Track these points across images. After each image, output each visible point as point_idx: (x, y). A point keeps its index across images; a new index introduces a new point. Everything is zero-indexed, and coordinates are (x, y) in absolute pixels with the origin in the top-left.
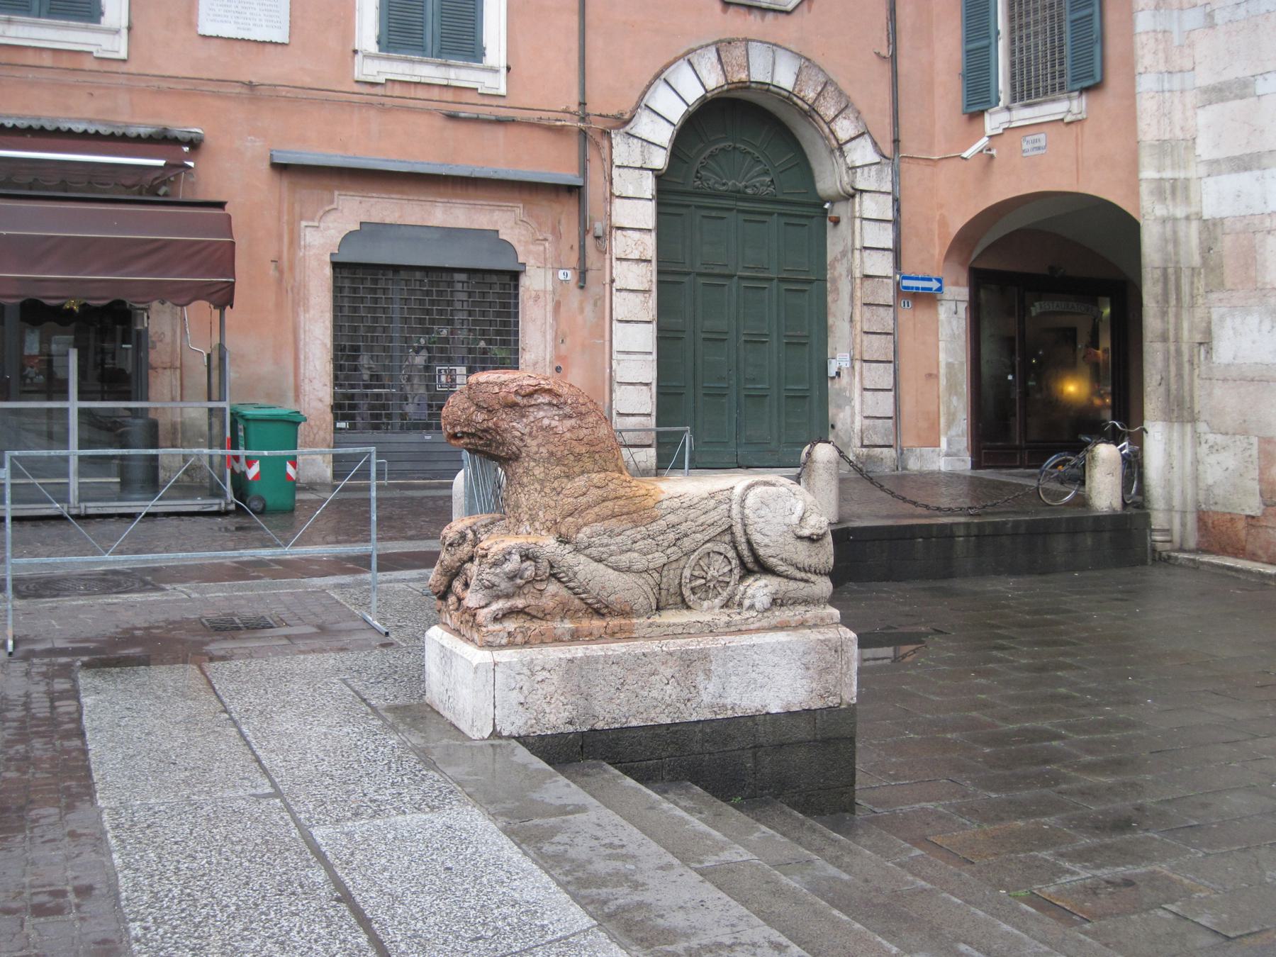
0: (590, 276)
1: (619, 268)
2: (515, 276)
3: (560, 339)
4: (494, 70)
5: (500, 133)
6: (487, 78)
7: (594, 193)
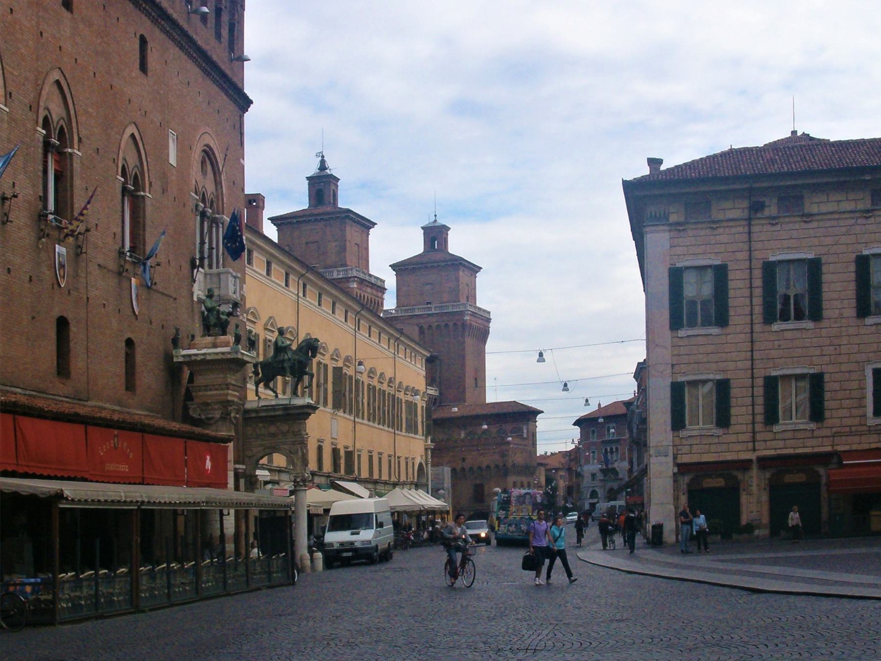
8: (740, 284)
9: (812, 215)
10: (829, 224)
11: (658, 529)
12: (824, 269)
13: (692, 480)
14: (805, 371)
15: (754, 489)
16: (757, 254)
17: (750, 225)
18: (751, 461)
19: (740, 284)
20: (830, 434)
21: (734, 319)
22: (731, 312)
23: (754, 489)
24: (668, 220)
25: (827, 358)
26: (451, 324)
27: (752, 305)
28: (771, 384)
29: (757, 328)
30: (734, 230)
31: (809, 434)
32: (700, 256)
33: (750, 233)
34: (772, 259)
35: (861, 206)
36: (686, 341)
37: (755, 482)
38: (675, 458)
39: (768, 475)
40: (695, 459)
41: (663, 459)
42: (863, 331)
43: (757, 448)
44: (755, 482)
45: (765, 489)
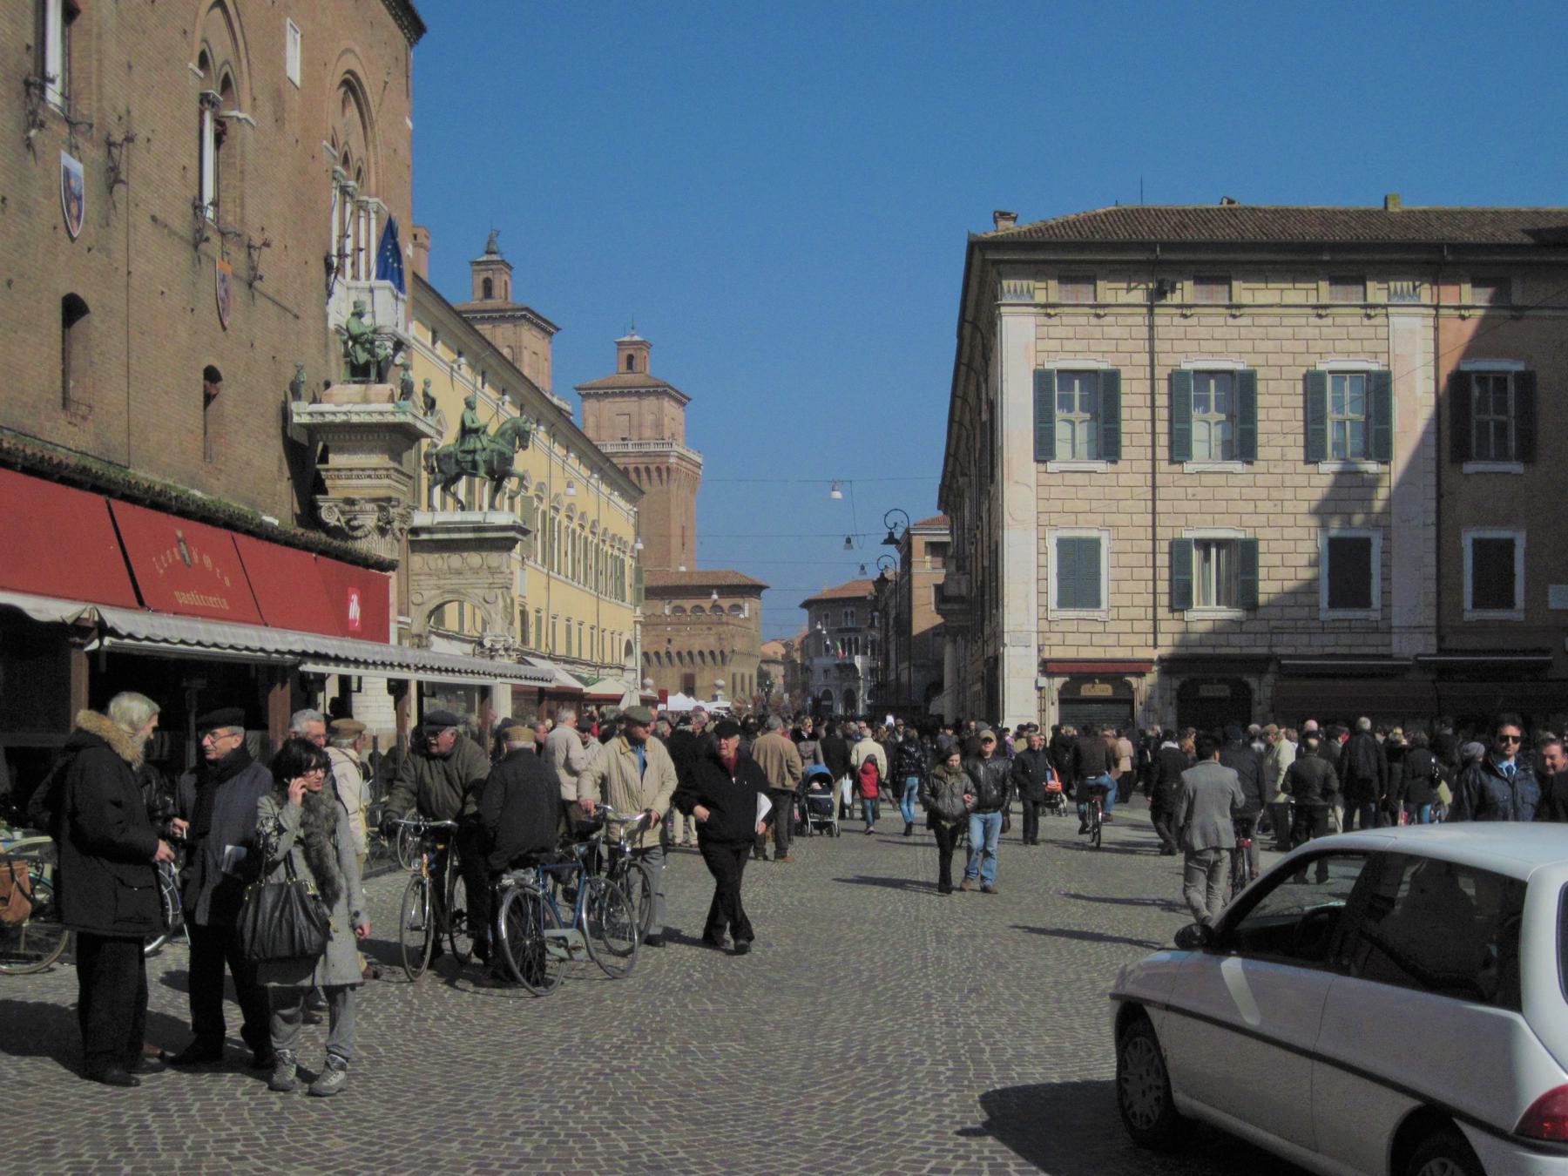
10: (1264, 321)
12: (1260, 387)
14: (1231, 534)
16: (1161, 359)
17: (1151, 314)
24: (1032, 297)
25: (1263, 518)
26: (653, 468)
28: (1180, 550)
29: (1163, 466)
30: (1130, 321)
32: (1079, 356)
33: (1151, 327)
34: (1186, 367)
36: (1058, 479)
39: (1176, 683)
40: (1070, 653)
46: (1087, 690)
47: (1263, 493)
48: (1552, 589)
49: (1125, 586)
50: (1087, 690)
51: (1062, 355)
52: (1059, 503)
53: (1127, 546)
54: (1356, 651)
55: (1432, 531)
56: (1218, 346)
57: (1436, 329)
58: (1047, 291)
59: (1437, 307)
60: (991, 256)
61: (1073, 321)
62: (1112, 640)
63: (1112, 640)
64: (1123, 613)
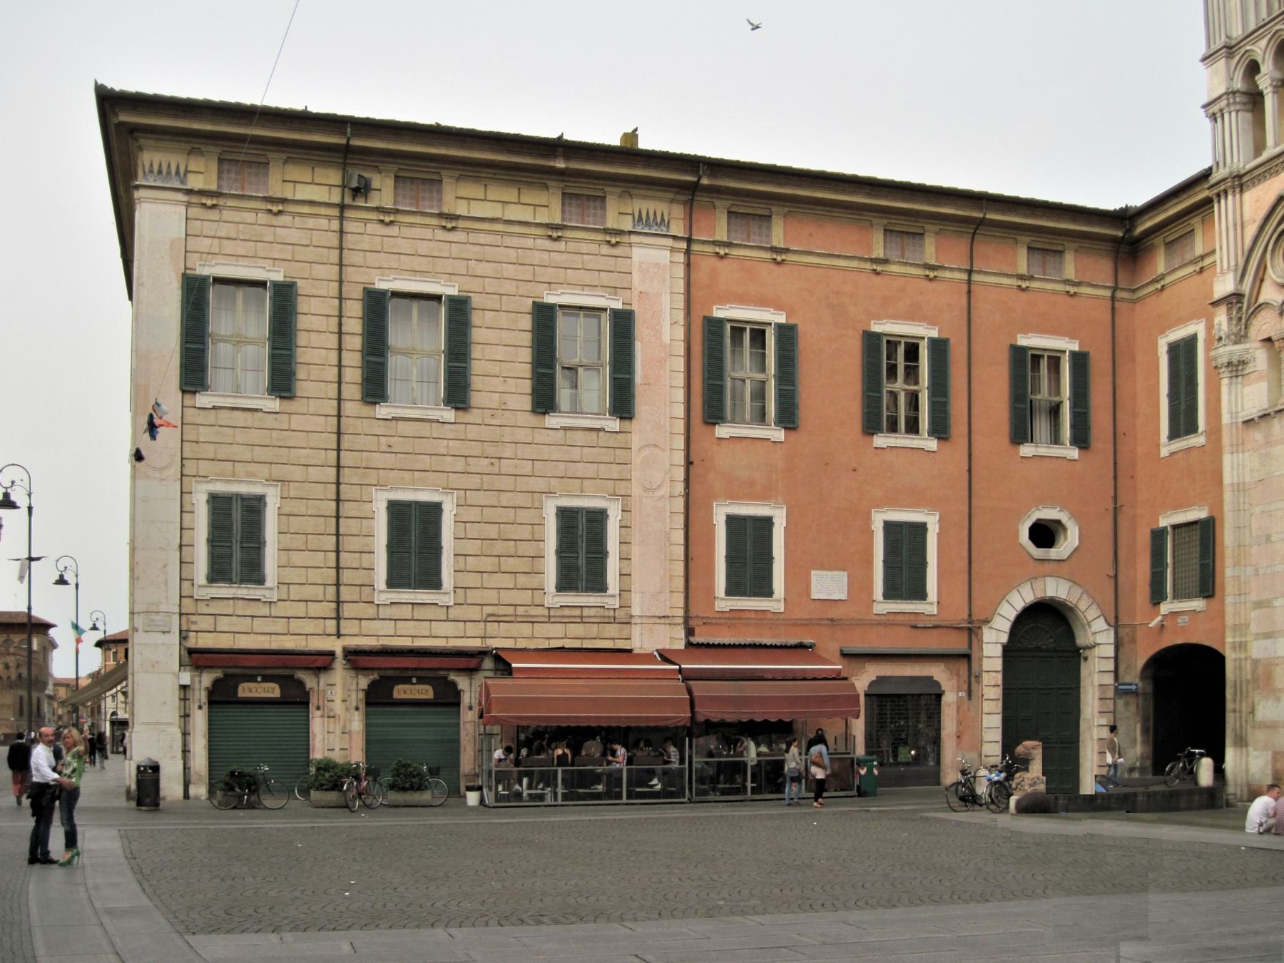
0: (974, 694)
1: (986, 690)
2: (939, 696)
3: (959, 723)
4: (931, 603)
5: (934, 632)
6: (928, 607)
7: (974, 656)
8: (319, 323)
9: (458, 217)
10: (483, 238)
11: (149, 776)
12: (476, 318)
13: (216, 683)
15: (338, 707)
16: (350, 273)
17: (342, 218)
18: (332, 654)
19: (319, 323)
20: (478, 617)
21: (303, 387)
22: (301, 373)
23: (338, 707)
25: (477, 479)
27: (340, 366)
29: (350, 408)
30: (311, 223)
31: (441, 614)
32: (242, 262)
35: (543, 217)
37: (338, 694)
38: (183, 636)
39: (364, 682)
40: (224, 642)
41: (160, 638)
42: (540, 437)
43: (342, 632)
44: (338, 694)
45: (357, 709)
46: (247, 690)
47: (476, 449)
48: (815, 575)
49: (298, 558)
50: (247, 690)
51: (221, 260)
52: (211, 448)
53: (300, 507)
54: (587, 644)
55: (680, 503)
56: (423, 264)
57: (688, 265)
58: (203, 174)
59: (689, 240)
60: (125, 117)
61: (237, 216)
62: (280, 626)
63: (280, 626)
64: (473, 596)
